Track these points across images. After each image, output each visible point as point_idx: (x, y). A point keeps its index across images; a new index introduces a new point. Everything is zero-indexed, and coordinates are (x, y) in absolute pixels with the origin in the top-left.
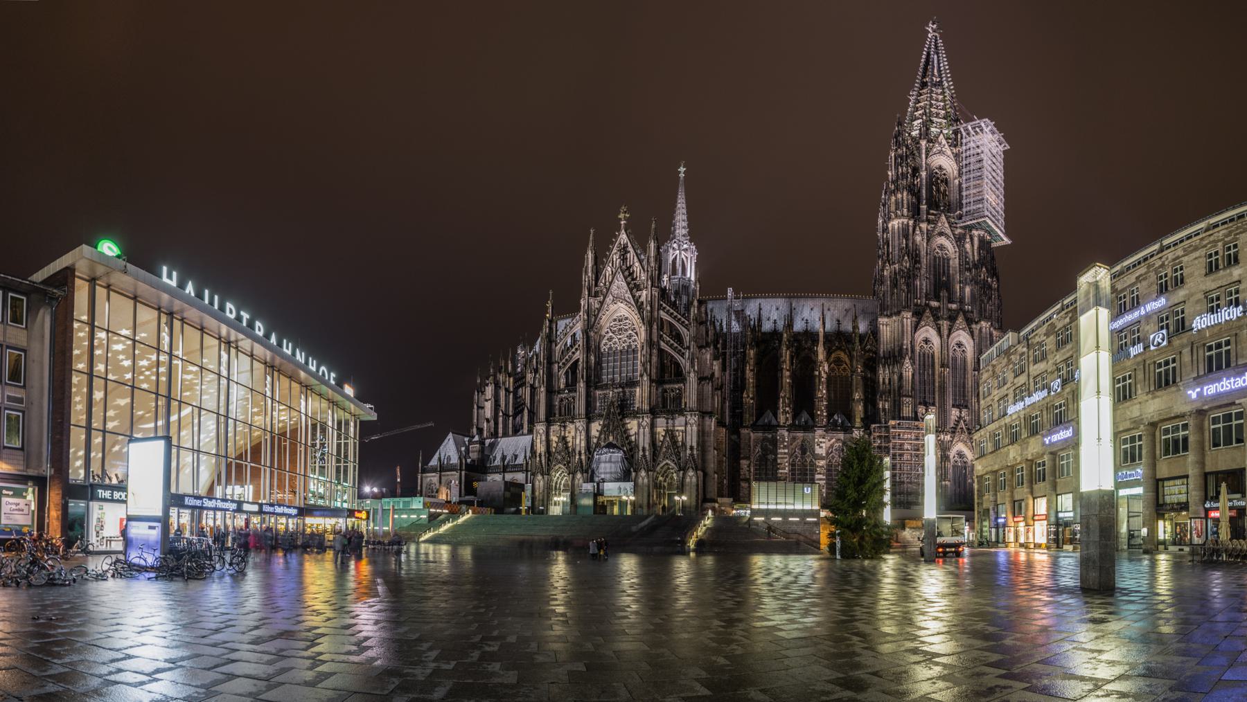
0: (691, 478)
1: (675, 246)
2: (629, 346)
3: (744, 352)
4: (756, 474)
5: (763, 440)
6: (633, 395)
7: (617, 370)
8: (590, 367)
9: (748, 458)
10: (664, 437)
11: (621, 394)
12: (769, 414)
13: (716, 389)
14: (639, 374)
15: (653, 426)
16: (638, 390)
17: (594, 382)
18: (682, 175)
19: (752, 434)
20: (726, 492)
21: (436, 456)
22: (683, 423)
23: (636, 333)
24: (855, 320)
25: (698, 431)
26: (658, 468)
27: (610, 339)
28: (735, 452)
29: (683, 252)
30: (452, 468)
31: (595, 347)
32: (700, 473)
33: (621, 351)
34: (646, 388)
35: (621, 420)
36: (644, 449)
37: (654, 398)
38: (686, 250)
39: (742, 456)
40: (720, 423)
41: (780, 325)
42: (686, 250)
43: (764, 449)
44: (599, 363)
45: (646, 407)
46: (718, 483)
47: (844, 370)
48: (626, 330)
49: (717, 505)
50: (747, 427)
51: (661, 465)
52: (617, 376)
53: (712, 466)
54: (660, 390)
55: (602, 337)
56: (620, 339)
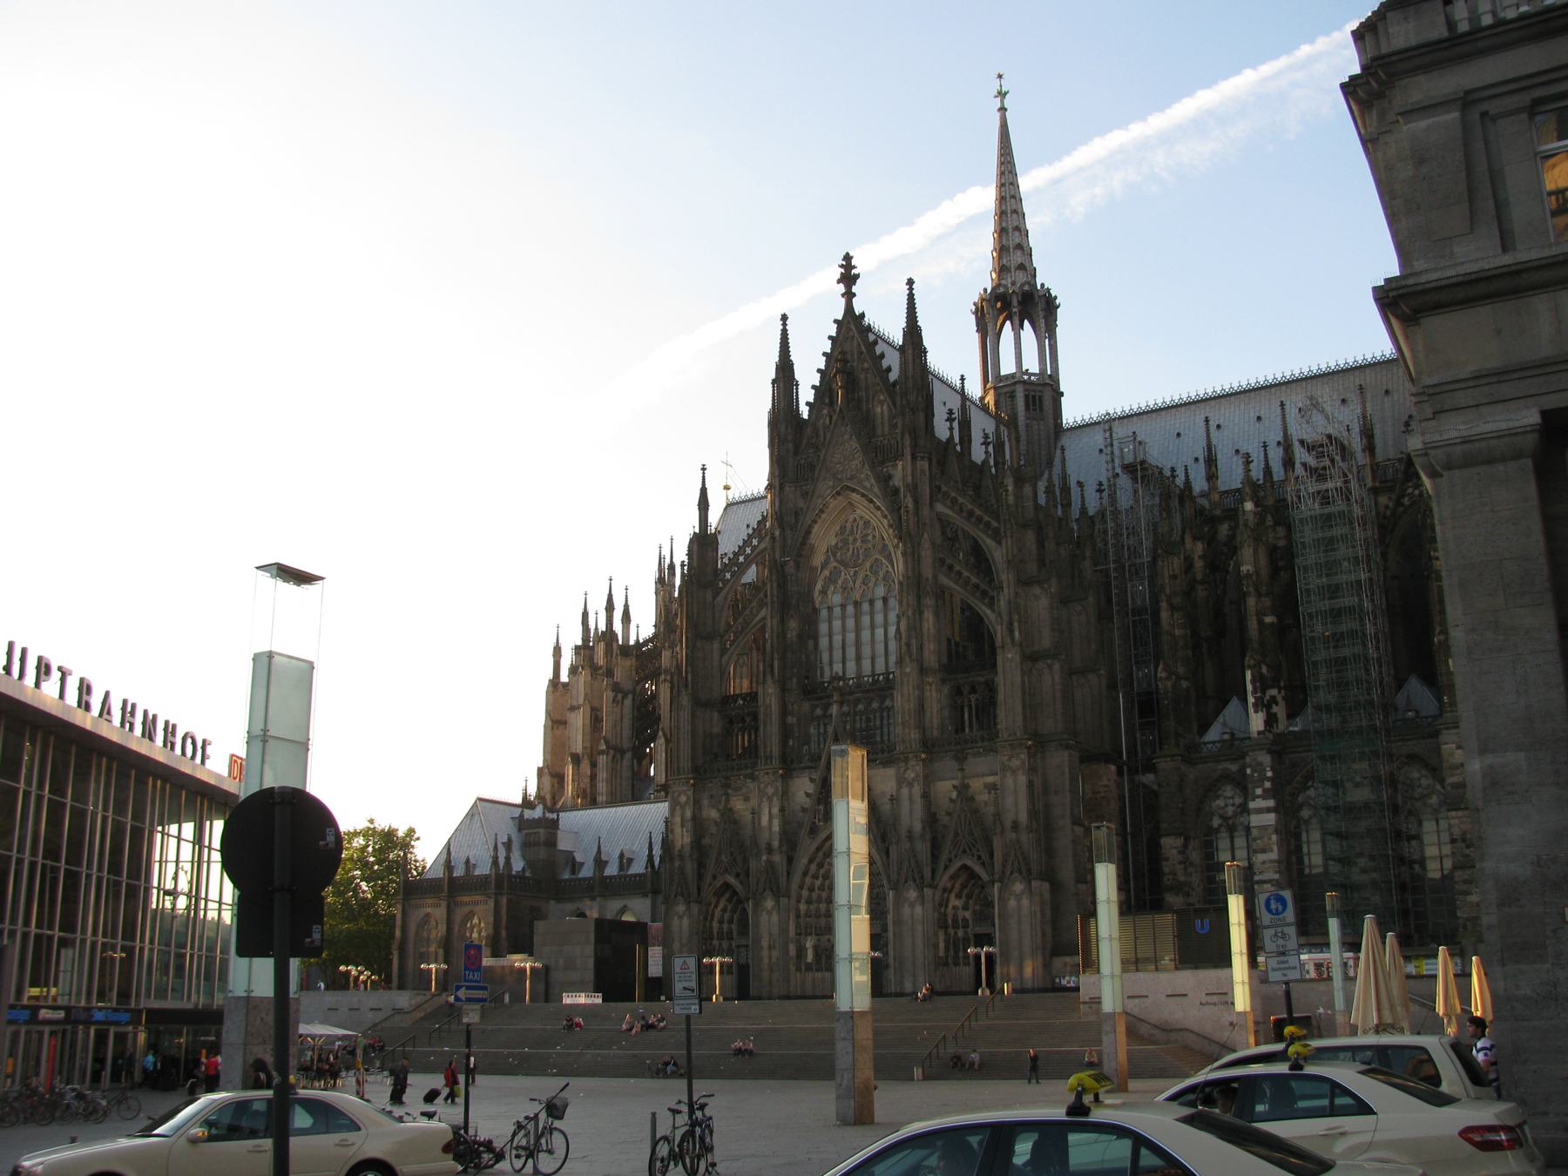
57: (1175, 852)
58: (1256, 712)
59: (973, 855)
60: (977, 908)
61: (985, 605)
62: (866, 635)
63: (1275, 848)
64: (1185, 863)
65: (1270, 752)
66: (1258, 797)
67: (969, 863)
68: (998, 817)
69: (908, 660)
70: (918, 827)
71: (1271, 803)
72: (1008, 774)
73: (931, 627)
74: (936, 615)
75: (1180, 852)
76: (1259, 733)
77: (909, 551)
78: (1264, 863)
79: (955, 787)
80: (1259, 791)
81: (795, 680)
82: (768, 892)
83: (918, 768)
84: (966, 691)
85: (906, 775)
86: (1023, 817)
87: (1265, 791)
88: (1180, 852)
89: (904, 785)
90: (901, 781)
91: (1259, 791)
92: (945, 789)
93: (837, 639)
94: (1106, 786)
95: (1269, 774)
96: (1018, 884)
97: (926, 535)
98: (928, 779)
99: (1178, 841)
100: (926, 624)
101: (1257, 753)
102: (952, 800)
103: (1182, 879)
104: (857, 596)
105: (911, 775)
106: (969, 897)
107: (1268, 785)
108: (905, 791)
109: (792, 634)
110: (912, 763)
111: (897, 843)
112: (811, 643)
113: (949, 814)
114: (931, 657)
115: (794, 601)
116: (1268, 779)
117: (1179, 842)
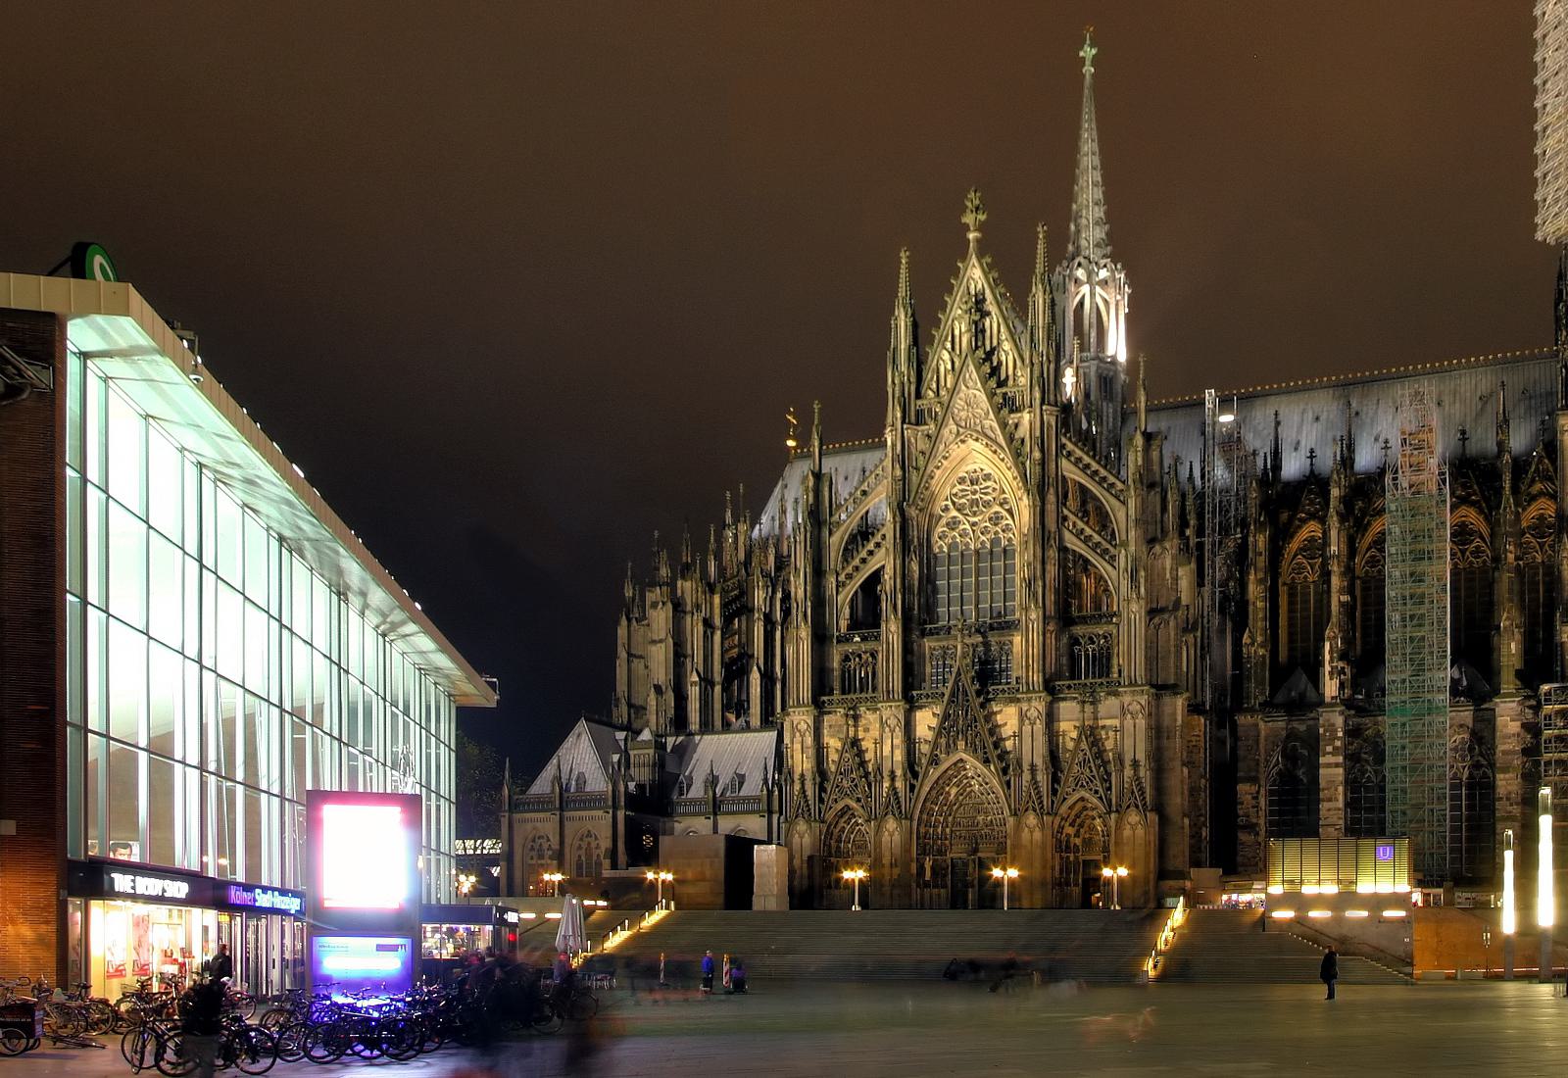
0: (1133, 828)
1: (1080, 273)
2: (995, 542)
3: (1245, 539)
4: (1272, 813)
5: (1288, 737)
6: (1005, 650)
7: (970, 594)
8: (911, 587)
9: (1254, 780)
10: (1078, 741)
11: (981, 649)
12: (1302, 680)
13: (1185, 630)
14: (1017, 603)
15: (1051, 718)
16: (1017, 639)
17: (919, 619)
18: (1089, 69)
19: (1262, 725)
20: (1206, 855)
21: (549, 771)
22: (1116, 710)
23: (1010, 512)
24: (1503, 425)
25: (1149, 727)
26: (1064, 809)
27: (953, 524)
28: (1224, 775)
29: (1098, 289)
30: (591, 801)
31: (921, 545)
32: (1153, 817)
33: (977, 552)
34: (1035, 637)
35: (983, 706)
36: (1033, 769)
37: (1052, 655)
38: (1104, 283)
39: (1240, 774)
40: (1195, 708)
41: (1327, 460)
42: (1104, 283)
43: (1291, 757)
44: (928, 579)
45: (1037, 678)
46: (1192, 837)
47: (1477, 552)
48: (987, 504)
49: (1188, 884)
50: (1252, 711)
51: (1070, 802)
52: (970, 608)
53: (1178, 800)
54: (1065, 640)
55: (934, 519)
56: (974, 524)
57: (1250, 797)
58: (1331, 679)
59: (1091, 790)
64: (1257, 807)
66: (1329, 753)
70: (1039, 762)
76: (1332, 698)
78: (1329, 810)
80: (1329, 749)
88: (1254, 798)
91: (1329, 749)
94: (1199, 736)
103: (1254, 821)
107: (1338, 743)
117: (1254, 789)
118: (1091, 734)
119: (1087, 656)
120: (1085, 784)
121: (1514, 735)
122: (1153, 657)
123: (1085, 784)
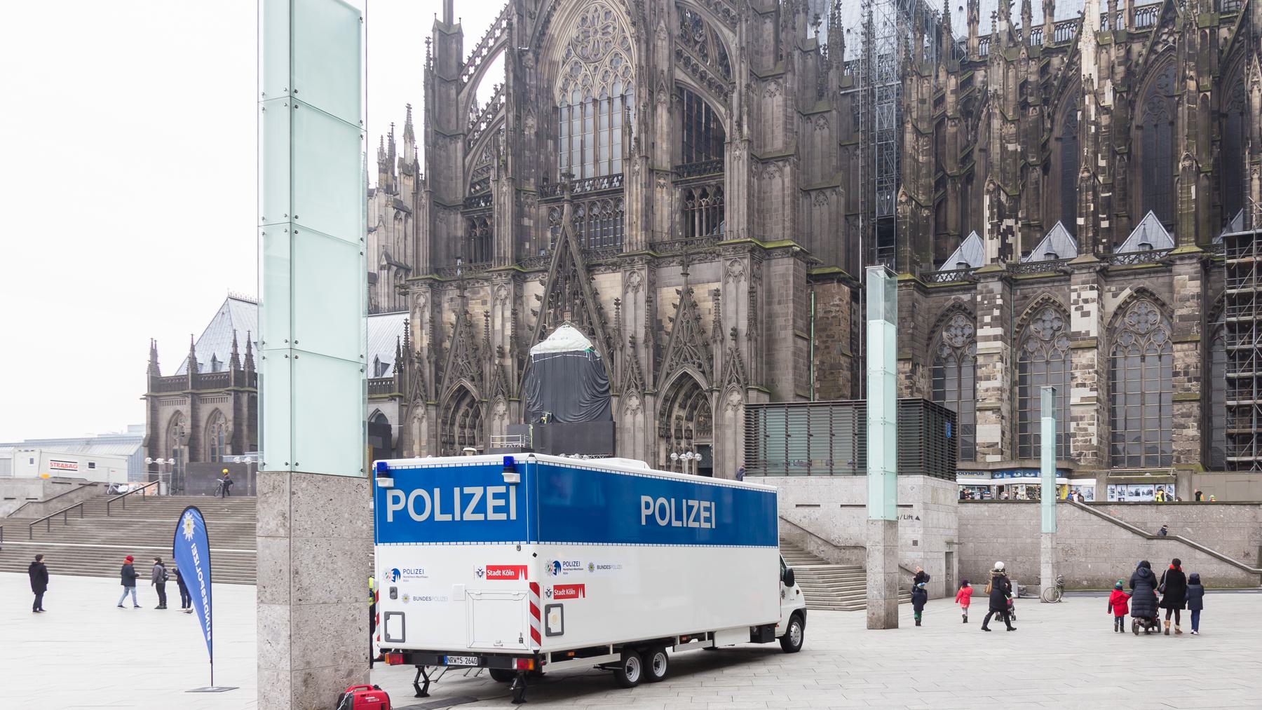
58: (991, 239)
60: (702, 419)
61: (720, 103)
62: (604, 135)
63: (999, 376)
64: (911, 388)
65: (1001, 279)
66: (987, 324)
67: (689, 372)
68: (718, 324)
69: (637, 156)
71: (999, 331)
72: (731, 280)
73: (665, 126)
74: (670, 111)
75: (907, 378)
76: (993, 260)
77: (644, 37)
78: (987, 390)
79: (678, 292)
80: (987, 319)
81: (532, 180)
82: (500, 396)
83: (643, 272)
84: (696, 194)
85: (632, 279)
86: (743, 326)
87: (994, 319)
88: (907, 378)
89: (630, 289)
90: (626, 286)
91: (987, 319)
92: (669, 296)
93: (577, 140)
94: (838, 305)
95: (999, 302)
96: (735, 394)
97: (662, 24)
98: (653, 286)
99: (907, 365)
100: (659, 121)
101: (989, 280)
102: (675, 306)
104: (596, 93)
105: (636, 279)
106: (693, 407)
107: (997, 312)
108: (630, 295)
109: (530, 132)
110: (638, 265)
111: (621, 350)
112: (550, 143)
113: (671, 320)
114: (663, 158)
115: (533, 97)
116: (998, 307)
118: (687, 300)
119: (701, 211)
120: (688, 356)
121: (1193, 297)
122: (757, 210)
123: (688, 356)
